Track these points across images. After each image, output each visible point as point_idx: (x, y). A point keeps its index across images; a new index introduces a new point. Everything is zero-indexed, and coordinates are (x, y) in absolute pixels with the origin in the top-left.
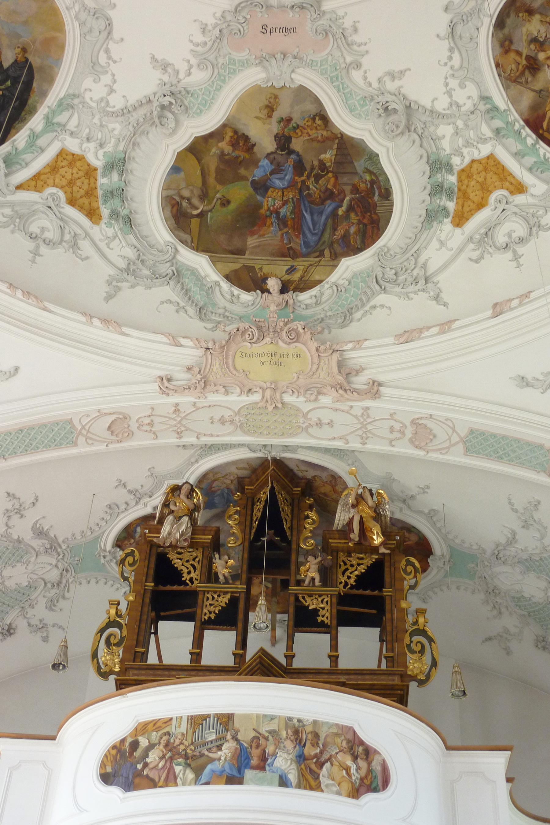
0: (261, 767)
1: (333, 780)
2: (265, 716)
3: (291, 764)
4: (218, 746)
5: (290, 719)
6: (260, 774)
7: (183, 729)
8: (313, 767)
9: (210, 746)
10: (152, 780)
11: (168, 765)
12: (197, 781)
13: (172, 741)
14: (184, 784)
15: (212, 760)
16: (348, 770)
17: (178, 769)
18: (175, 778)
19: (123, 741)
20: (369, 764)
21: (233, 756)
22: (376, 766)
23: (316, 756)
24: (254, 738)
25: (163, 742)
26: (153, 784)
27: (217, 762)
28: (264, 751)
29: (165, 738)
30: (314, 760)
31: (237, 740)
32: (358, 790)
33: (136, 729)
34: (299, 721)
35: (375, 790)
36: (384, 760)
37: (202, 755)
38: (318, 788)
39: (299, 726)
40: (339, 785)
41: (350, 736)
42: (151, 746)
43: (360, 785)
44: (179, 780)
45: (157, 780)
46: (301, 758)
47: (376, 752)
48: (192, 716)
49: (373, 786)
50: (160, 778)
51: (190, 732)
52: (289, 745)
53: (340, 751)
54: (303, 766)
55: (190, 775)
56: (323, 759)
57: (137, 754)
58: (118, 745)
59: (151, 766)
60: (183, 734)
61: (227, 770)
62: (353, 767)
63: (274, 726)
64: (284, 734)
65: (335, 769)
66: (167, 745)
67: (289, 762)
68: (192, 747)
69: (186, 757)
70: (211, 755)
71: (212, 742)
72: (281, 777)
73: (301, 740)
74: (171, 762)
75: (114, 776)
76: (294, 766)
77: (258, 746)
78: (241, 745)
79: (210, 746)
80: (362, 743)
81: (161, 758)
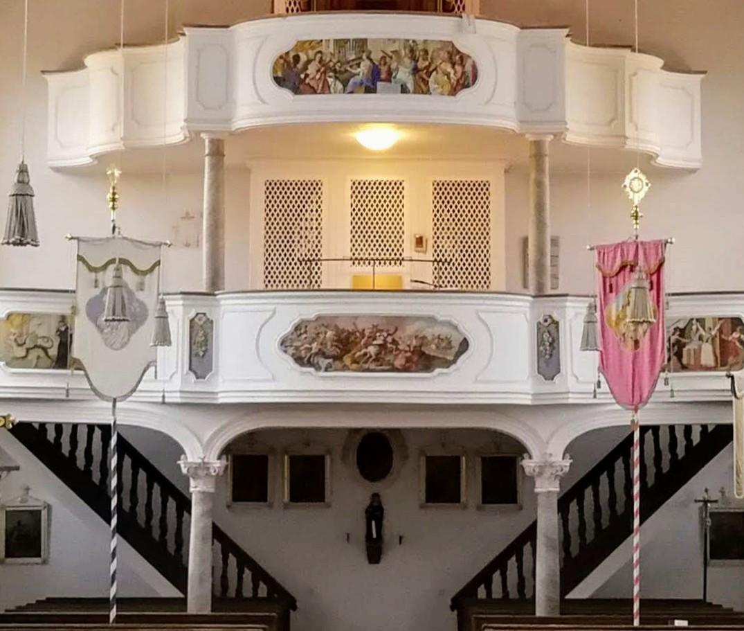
0: (388, 80)
1: (438, 84)
2: (389, 40)
3: (408, 77)
4: (357, 64)
5: (407, 41)
6: (388, 84)
7: (331, 49)
8: (425, 76)
9: (351, 64)
10: (313, 88)
11: (323, 77)
12: (344, 91)
13: (324, 58)
14: (335, 92)
15: (354, 75)
16: (448, 75)
17: (330, 80)
18: (329, 87)
19: (287, 53)
20: (463, 66)
21: (368, 72)
22: (468, 68)
23: (427, 67)
24: (384, 58)
25: (317, 59)
26: (314, 92)
27: (357, 77)
28: (389, 68)
29: (319, 55)
30: (425, 71)
31: (371, 60)
32: (455, 89)
33: (296, 46)
34: (414, 41)
35: (468, 86)
36: (474, 62)
37: (346, 71)
38: (428, 92)
39: (414, 46)
40: (442, 87)
41: (450, 49)
42: (309, 62)
43: (457, 85)
44: (332, 90)
45: (316, 88)
46: (416, 70)
47: (469, 57)
48: (336, 40)
49: (466, 83)
50: (318, 86)
51: (337, 51)
52: (407, 61)
53: (443, 61)
54: (417, 77)
55: (340, 86)
56: (431, 69)
57: (300, 66)
58: (284, 56)
59: (311, 76)
60: (331, 54)
61: (365, 81)
62: (452, 72)
63: (395, 47)
64: (403, 53)
65: (440, 74)
66: (320, 62)
67: (407, 74)
68: (339, 64)
69: (335, 71)
70: (353, 71)
71: (353, 60)
72: (402, 86)
73: (415, 56)
74: (325, 74)
75: (284, 80)
76: (411, 77)
77: (385, 64)
78: (374, 64)
79: (351, 64)
80: (459, 52)
81: (318, 71)
